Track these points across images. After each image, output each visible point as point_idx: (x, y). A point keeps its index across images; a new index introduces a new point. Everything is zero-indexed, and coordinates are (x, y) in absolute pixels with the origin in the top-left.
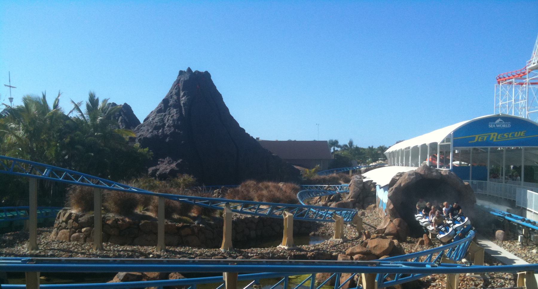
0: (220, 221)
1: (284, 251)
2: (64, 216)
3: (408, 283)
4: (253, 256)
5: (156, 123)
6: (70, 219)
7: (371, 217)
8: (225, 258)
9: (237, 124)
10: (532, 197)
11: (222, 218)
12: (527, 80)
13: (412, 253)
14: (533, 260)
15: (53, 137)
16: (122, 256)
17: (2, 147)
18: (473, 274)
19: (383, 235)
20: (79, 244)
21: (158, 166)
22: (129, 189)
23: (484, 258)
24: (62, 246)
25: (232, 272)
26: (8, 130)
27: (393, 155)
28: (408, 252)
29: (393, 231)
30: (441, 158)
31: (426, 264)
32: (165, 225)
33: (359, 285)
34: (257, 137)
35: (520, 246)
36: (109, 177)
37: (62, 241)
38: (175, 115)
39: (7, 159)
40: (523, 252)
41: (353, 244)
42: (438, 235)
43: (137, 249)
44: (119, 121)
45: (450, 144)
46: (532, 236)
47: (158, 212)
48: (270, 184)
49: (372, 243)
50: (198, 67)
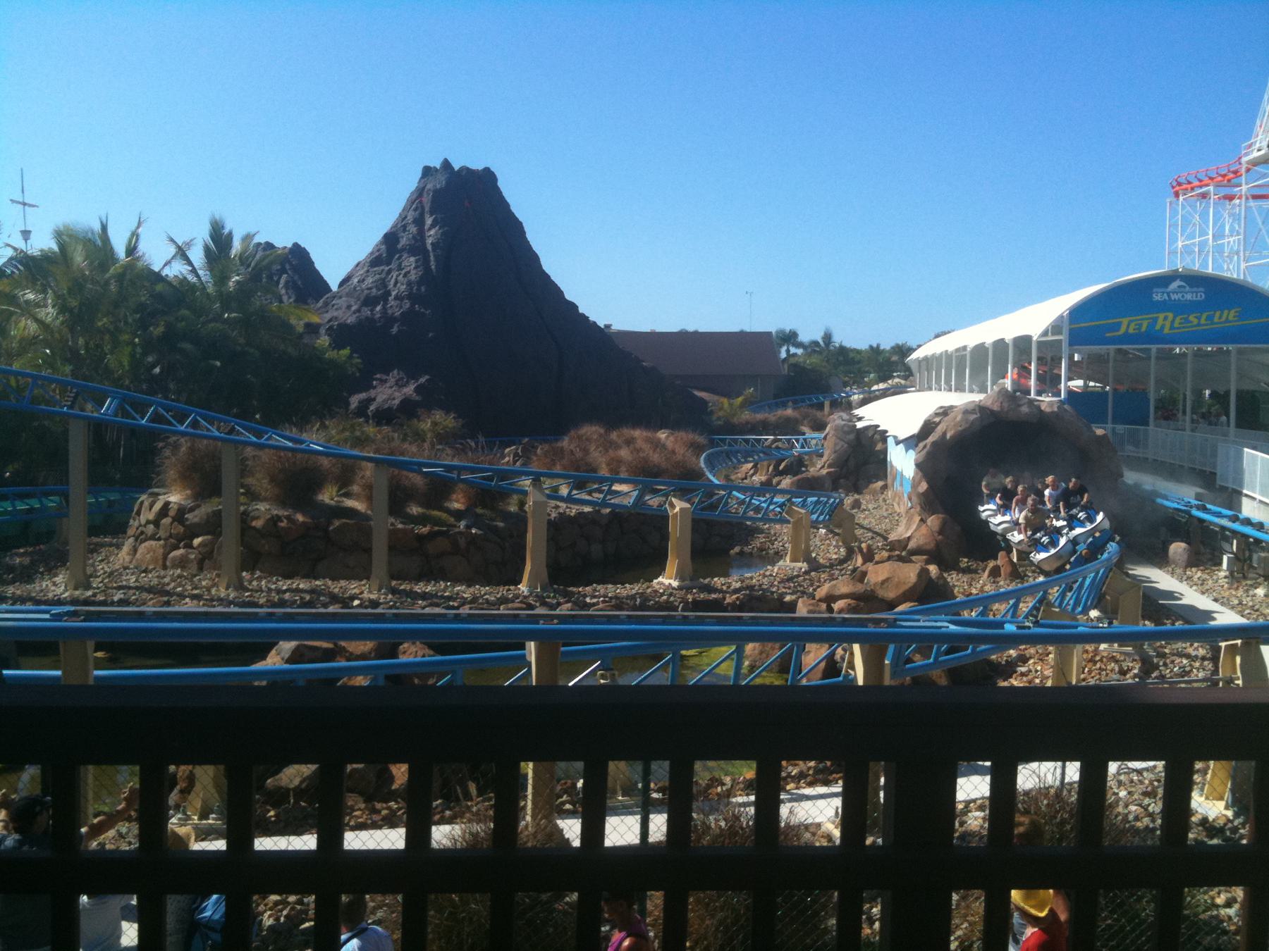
0: (519, 521)
1: (670, 590)
2: (150, 510)
3: (962, 667)
4: (597, 603)
5: (368, 289)
6: (166, 515)
7: (874, 512)
8: (531, 607)
9: (558, 292)
10: (1255, 464)
11: (523, 514)
12: (1244, 188)
13: (971, 597)
14: (1258, 613)
15: (126, 323)
16: (288, 603)
17: (4, 347)
18: (1116, 645)
19: (904, 554)
20: (185, 574)
21: (372, 390)
22: (303, 446)
23: (1143, 609)
24: (145, 579)
25: (547, 641)
26: (18, 305)
27: (927, 366)
28: (963, 594)
29: (926, 544)
30: (1040, 372)
31: (1004, 623)
32: (390, 531)
33: (847, 672)
34: (607, 323)
35: (1226, 580)
36: (258, 416)
37: (147, 568)
38: (413, 272)
39: (17, 374)
40: (1234, 593)
41: (833, 574)
42: (1032, 555)
43: (323, 587)
44: (281, 286)
45: (1061, 340)
46: (1255, 557)
47: (372, 500)
48: (637, 433)
49: (877, 574)
50: (467, 158)
